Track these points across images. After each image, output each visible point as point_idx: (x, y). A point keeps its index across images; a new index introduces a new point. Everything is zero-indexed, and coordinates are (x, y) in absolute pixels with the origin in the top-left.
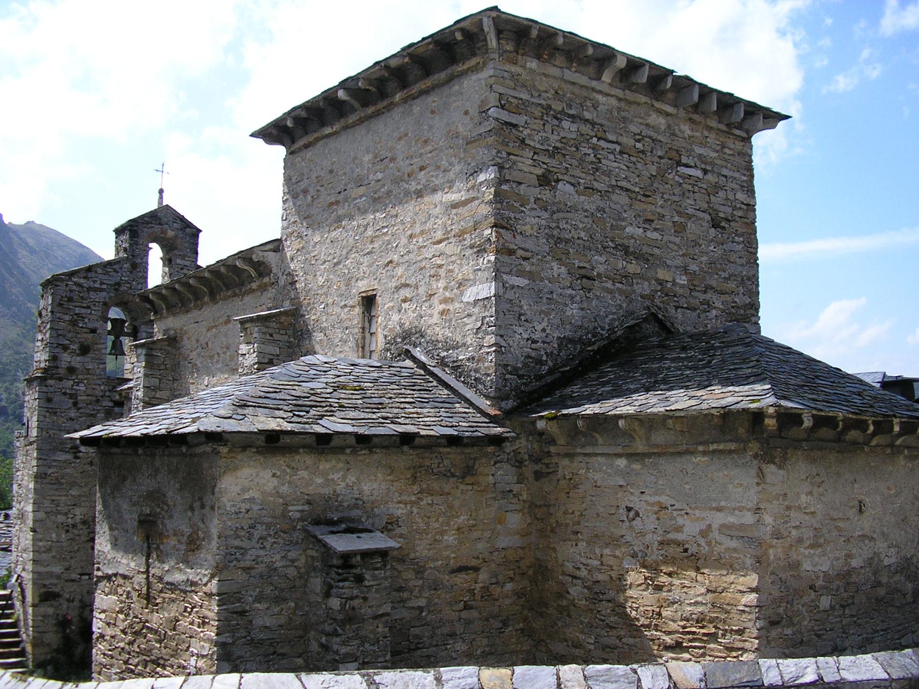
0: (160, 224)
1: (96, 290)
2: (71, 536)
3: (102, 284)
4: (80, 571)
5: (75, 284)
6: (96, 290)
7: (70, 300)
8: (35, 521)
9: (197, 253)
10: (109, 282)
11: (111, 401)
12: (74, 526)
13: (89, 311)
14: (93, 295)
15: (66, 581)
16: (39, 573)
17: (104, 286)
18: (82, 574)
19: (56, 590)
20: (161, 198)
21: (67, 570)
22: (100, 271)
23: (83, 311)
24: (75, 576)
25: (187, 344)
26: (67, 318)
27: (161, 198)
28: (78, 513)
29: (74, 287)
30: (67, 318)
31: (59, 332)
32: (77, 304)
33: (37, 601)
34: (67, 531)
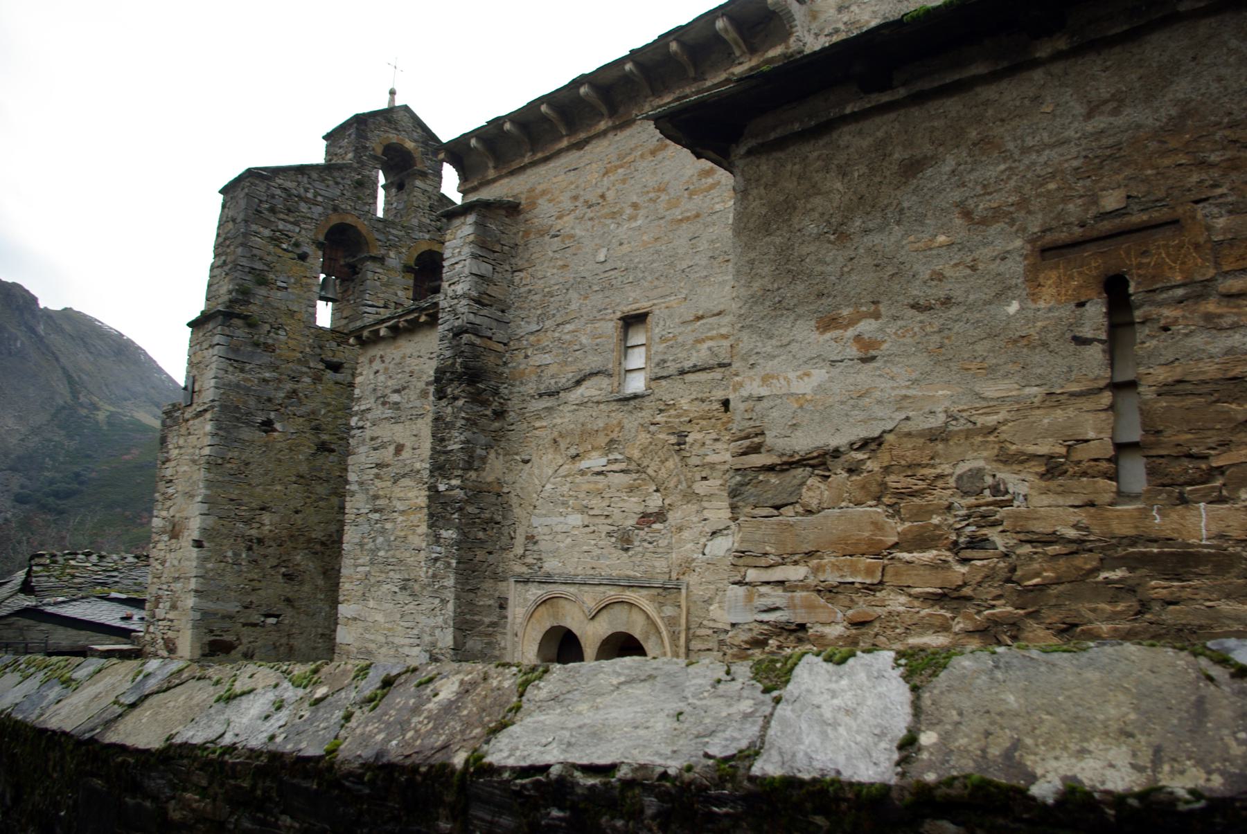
0: (396, 129)
1: (306, 200)
2: (255, 556)
3: (316, 194)
4: (264, 609)
5: (280, 187)
6: (306, 200)
7: (272, 210)
8: (204, 530)
9: (441, 178)
10: (326, 194)
11: (322, 360)
12: (260, 541)
13: (297, 229)
14: (303, 207)
15: (244, 625)
16: (205, 614)
17: (320, 199)
18: (268, 616)
19: (228, 638)
20: (392, 100)
21: (246, 607)
22: (315, 175)
23: (290, 227)
24: (256, 618)
25: (544, 213)
26: (267, 233)
27: (392, 100)
28: (267, 522)
29: (278, 192)
30: (267, 233)
31: (255, 251)
32: (282, 216)
33: (197, 656)
34: (250, 549)
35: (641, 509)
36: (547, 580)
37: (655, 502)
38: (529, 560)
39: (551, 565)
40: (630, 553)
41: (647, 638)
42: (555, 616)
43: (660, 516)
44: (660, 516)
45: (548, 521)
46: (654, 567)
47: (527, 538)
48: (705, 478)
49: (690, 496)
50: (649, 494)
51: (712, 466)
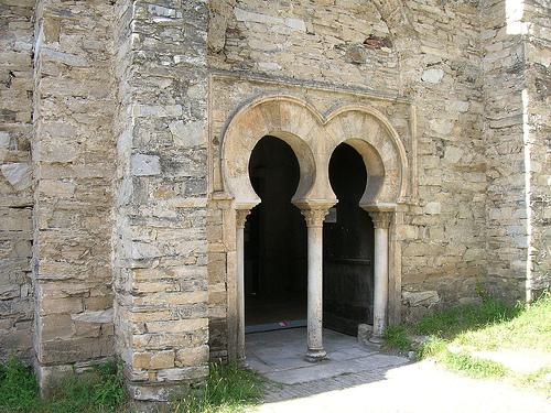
35: (369, 31)
36: (265, 78)
37: (382, 30)
38: (233, 56)
39: (264, 66)
40: (362, 68)
41: (381, 144)
42: (276, 121)
43: (387, 42)
44: (387, 42)
45: (262, 19)
46: (386, 84)
47: (228, 31)
48: (419, 21)
49: (411, 32)
50: (377, 21)
51: (426, 14)
